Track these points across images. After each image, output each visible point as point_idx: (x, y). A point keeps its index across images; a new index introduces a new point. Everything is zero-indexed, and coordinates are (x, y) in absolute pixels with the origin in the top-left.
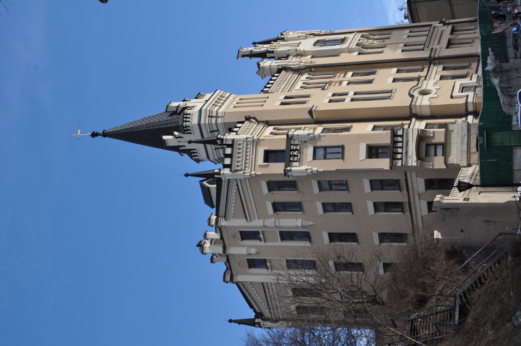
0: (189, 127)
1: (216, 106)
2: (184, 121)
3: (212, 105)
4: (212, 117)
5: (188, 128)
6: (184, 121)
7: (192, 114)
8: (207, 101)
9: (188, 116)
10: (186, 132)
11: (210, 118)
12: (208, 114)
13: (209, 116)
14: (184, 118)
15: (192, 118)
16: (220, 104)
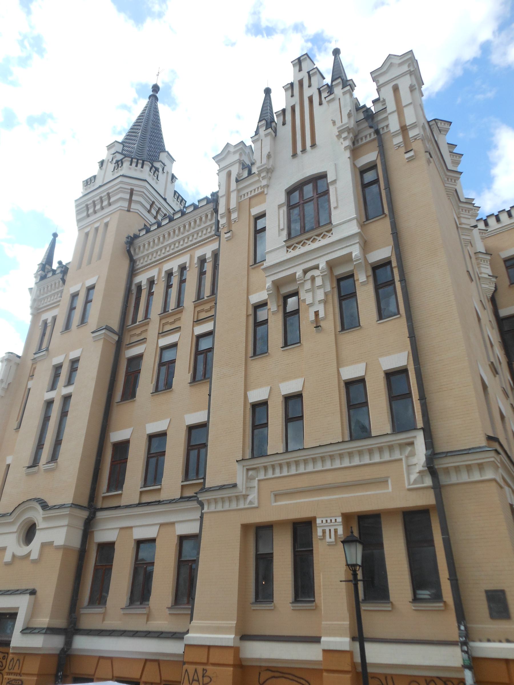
0: (122, 165)
1: (151, 206)
2: (132, 159)
3: (153, 200)
4: (131, 194)
5: (120, 166)
6: (132, 159)
7: (141, 171)
8: (165, 200)
9: (140, 166)
10: (116, 164)
11: (129, 191)
12: (135, 188)
13: (132, 191)
14: (138, 160)
15: (136, 170)
16: (154, 212)
